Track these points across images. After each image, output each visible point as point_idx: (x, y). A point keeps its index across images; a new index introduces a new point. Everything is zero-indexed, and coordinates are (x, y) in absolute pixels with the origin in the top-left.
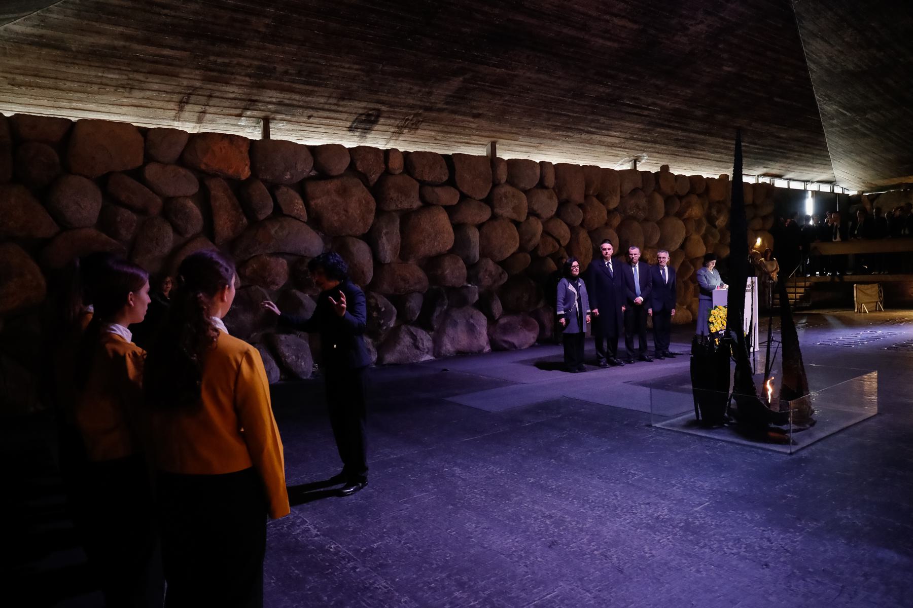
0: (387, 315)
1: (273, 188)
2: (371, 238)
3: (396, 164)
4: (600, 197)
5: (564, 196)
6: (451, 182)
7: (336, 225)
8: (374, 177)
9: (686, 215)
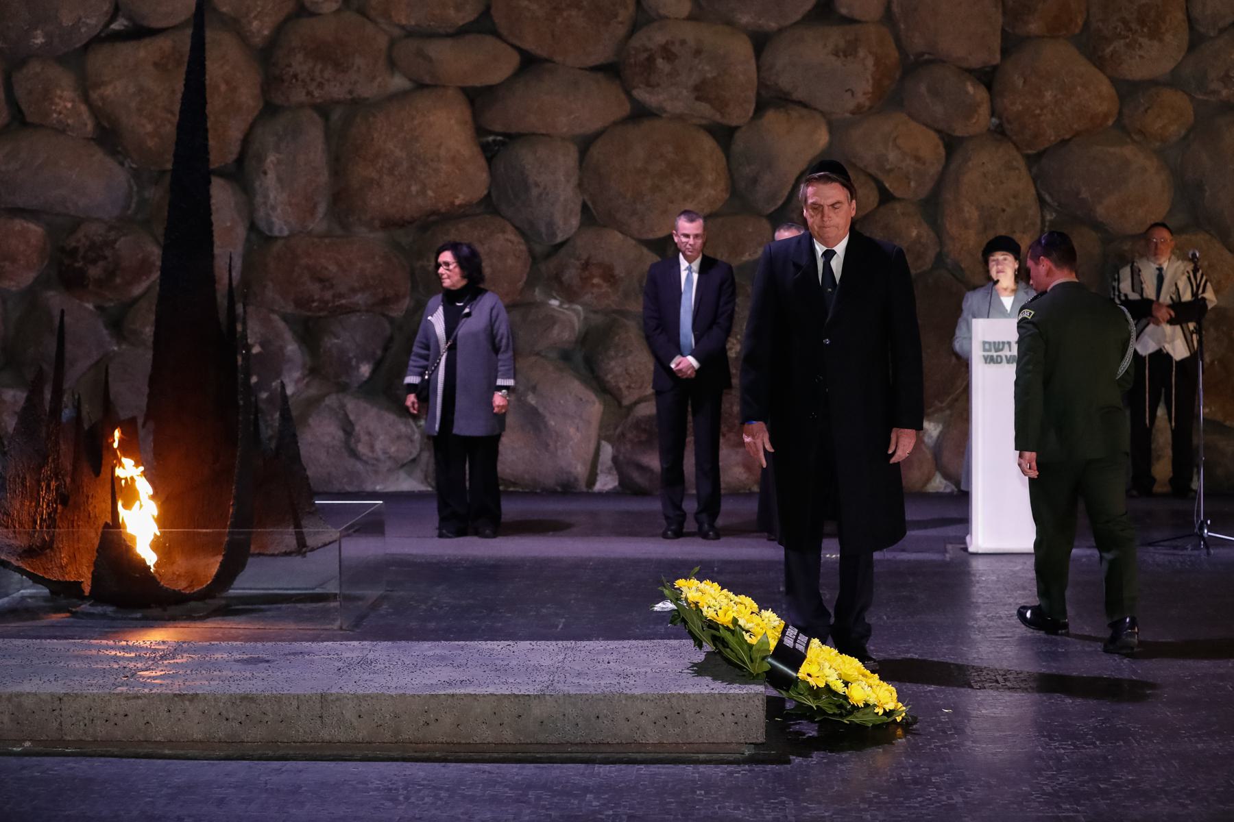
0: (272, 362)
5: (918, 43)
6: (483, 25)
7: (150, 143)
8: (260, 28)
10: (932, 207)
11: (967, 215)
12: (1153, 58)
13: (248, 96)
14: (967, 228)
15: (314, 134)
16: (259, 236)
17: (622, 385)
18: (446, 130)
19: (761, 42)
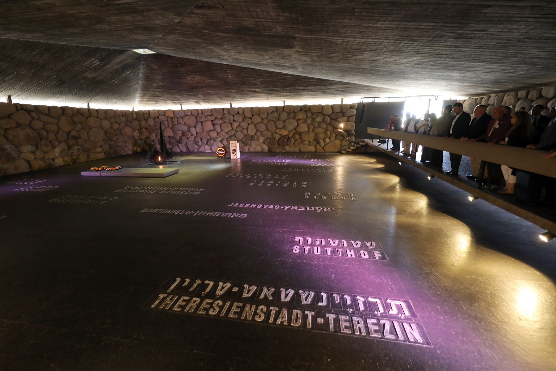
0: (198, 142)
1: (178, 118)
2: (195, 127)
3: (200, 112)
4: (259, 115)
6: (212, 115)
8: (196, 115)
9: (297, 118)
10: (247, 129)
12: (264, 116)
13: (195, 121)
15: (200, 124)
16: (197, 133)
18: (210, 123)
19: (233, 116)
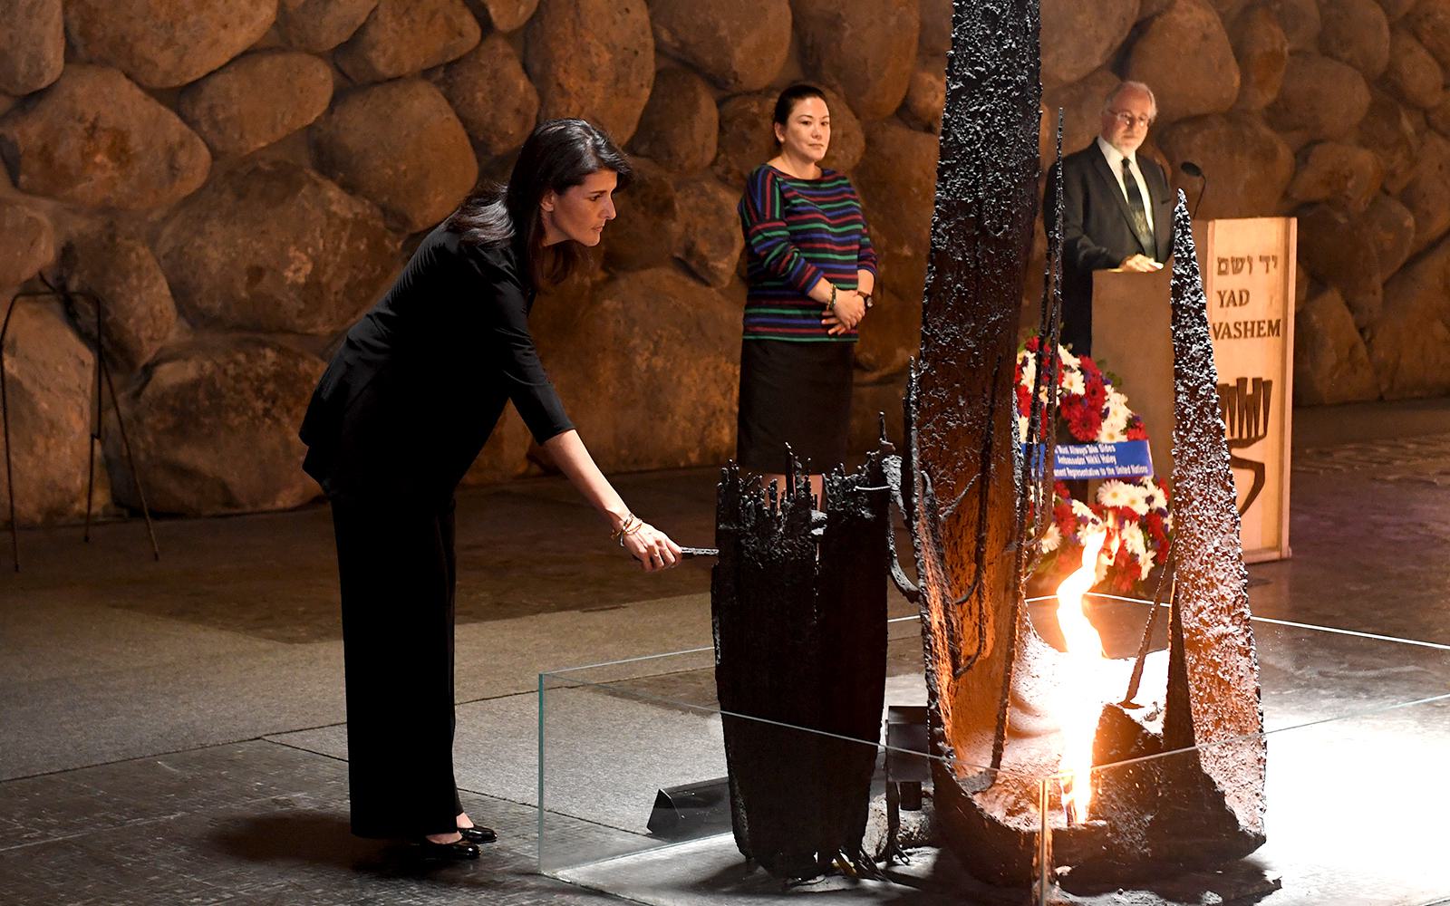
11: (595, 60)
14: (593, 79)
17: (144, 335)
